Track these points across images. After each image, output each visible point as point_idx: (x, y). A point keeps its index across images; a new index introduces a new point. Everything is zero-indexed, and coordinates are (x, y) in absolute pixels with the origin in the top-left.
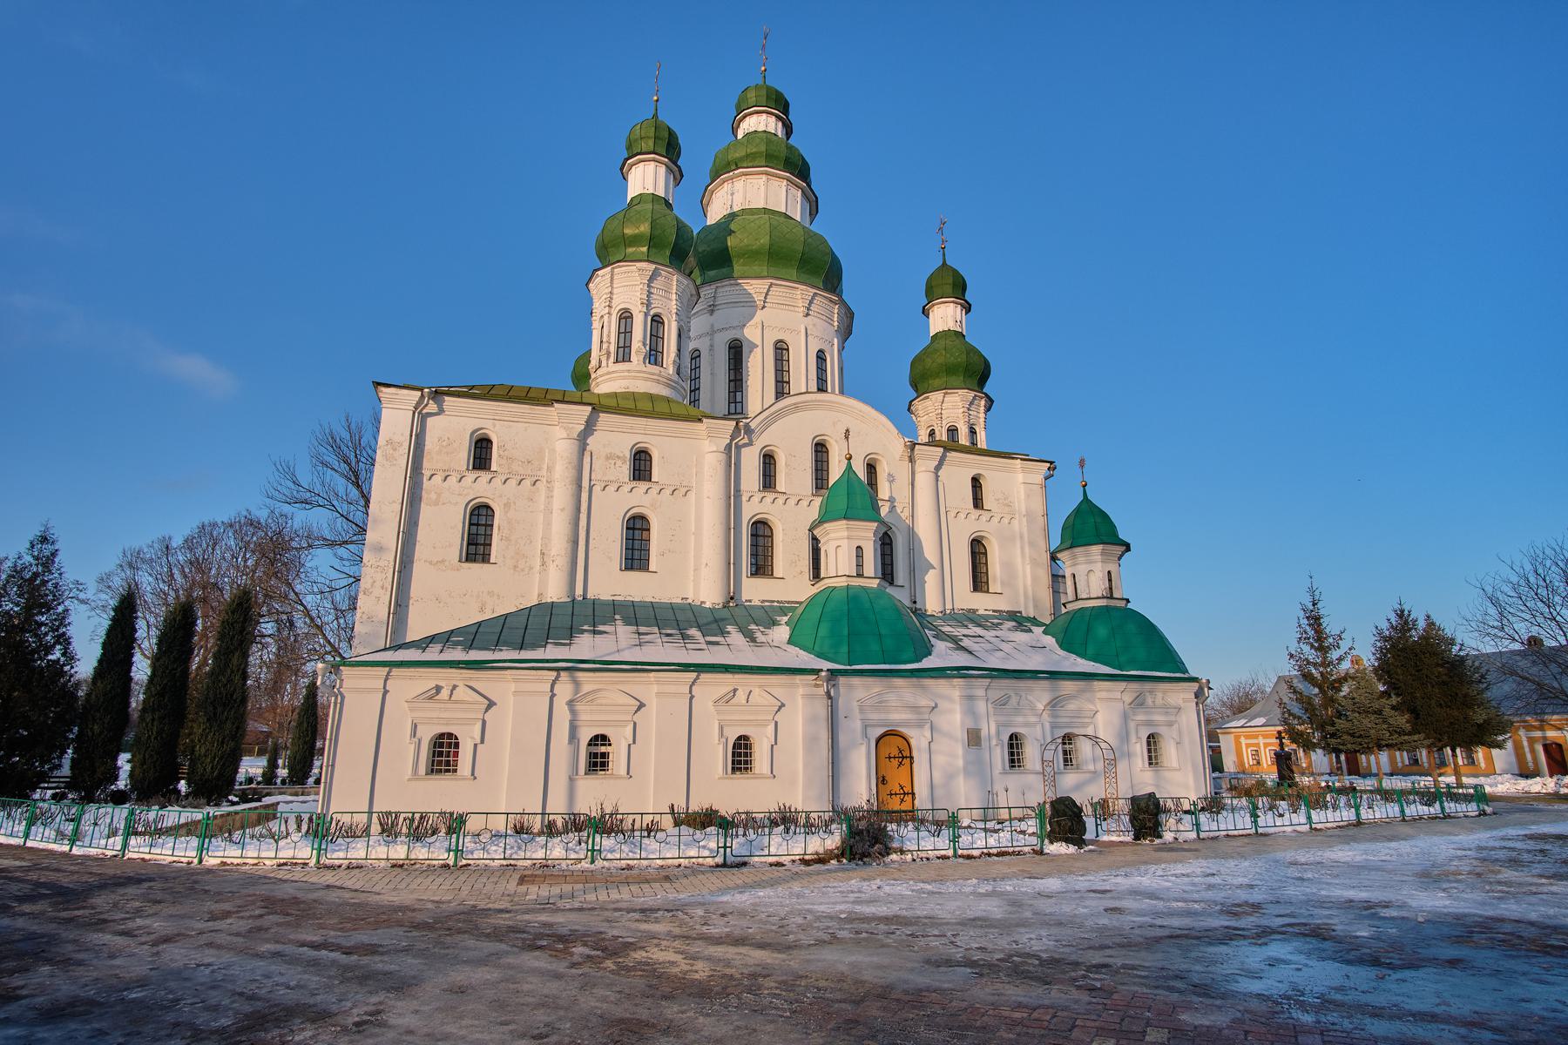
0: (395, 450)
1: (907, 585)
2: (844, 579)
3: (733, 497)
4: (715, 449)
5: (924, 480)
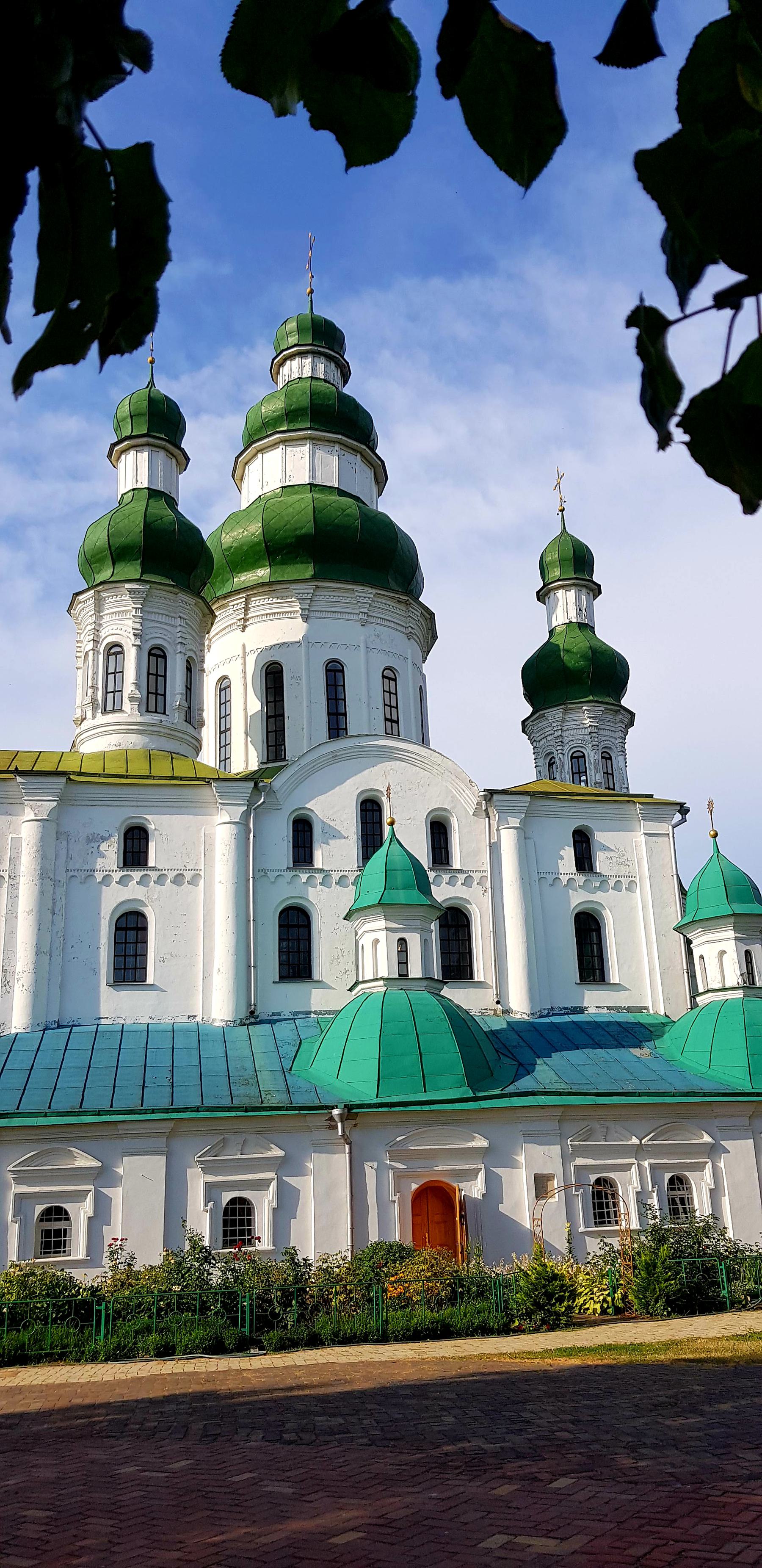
2: (381, 983)
4: (228, 820)
5: (508, 840)
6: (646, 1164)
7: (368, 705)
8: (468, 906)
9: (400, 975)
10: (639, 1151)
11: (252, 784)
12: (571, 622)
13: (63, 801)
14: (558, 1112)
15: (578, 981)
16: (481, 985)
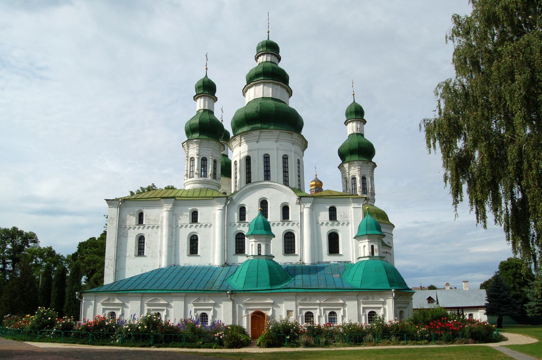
0: (113, 220)
1: (299, 254)
2: (252, 257)
3: (227, 224)
5: (306, 212)
6: (322, 308)
7: (277, 168)
8: (293, 232)
9: (258, 254)
10: (320, 305)
11: (226, 198)
12: (354, 133)
13: (174, 205)
14: (295, 294)
15: (328, 254)
16: (297, 255)
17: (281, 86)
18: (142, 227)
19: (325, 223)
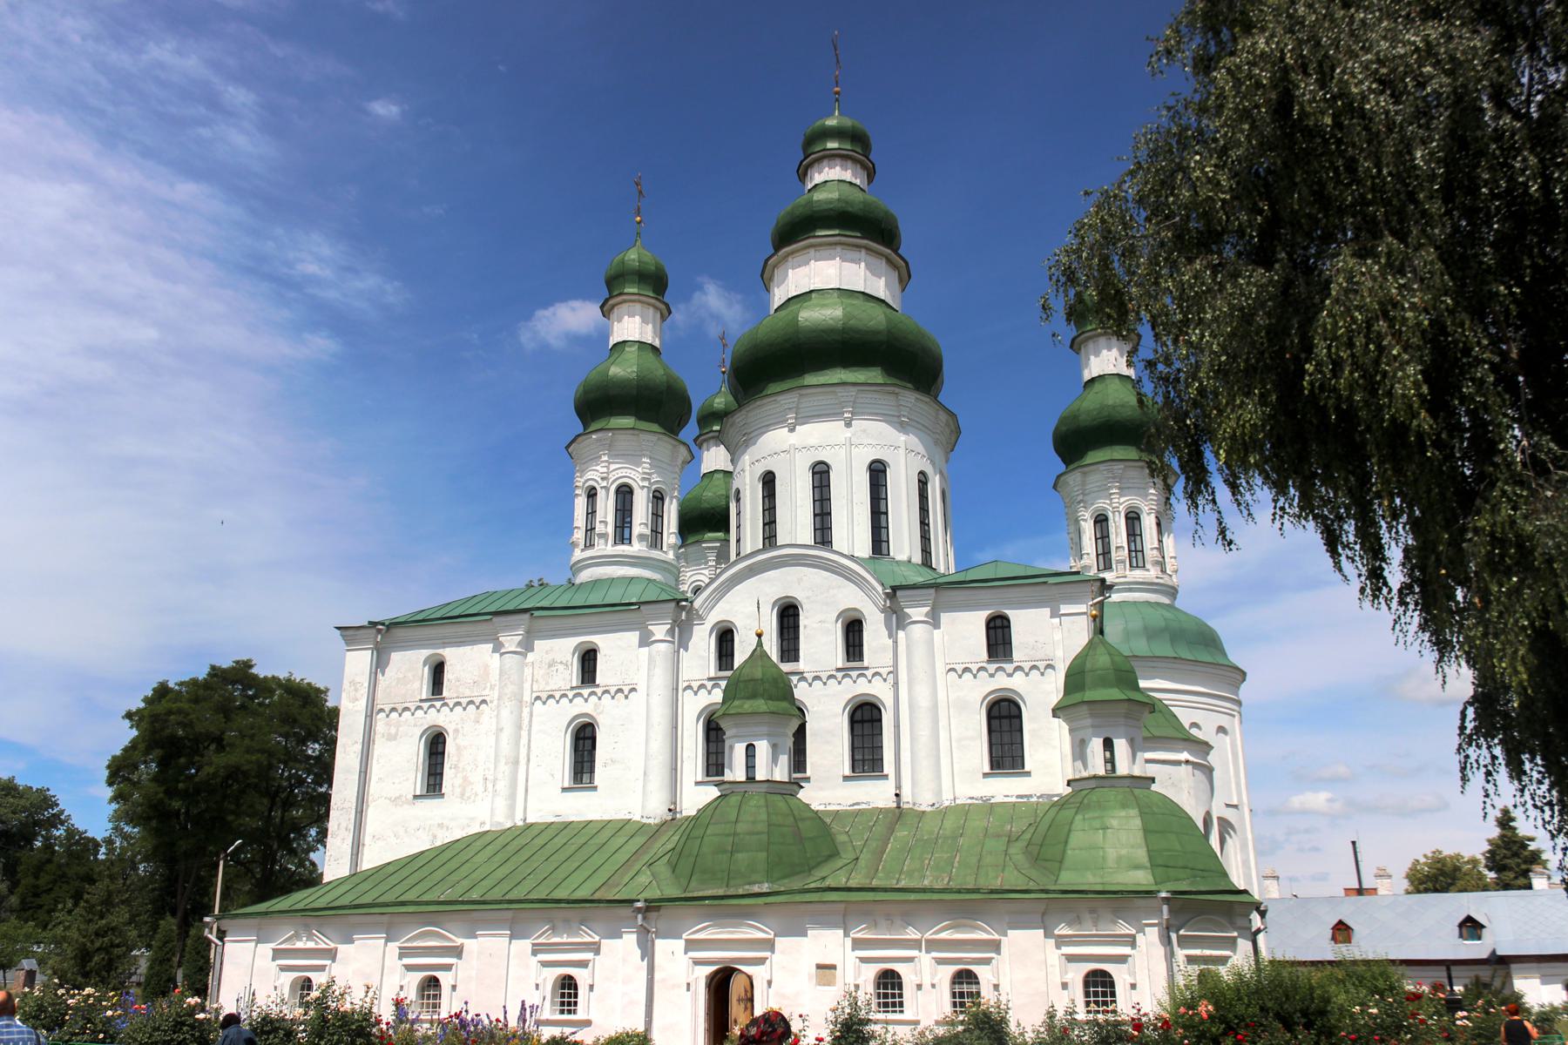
9: (748, 778)
11: (673, 605)
15: (987, 769)
17: (868, 249)
18: (438, 704)
19: (974, 668)
